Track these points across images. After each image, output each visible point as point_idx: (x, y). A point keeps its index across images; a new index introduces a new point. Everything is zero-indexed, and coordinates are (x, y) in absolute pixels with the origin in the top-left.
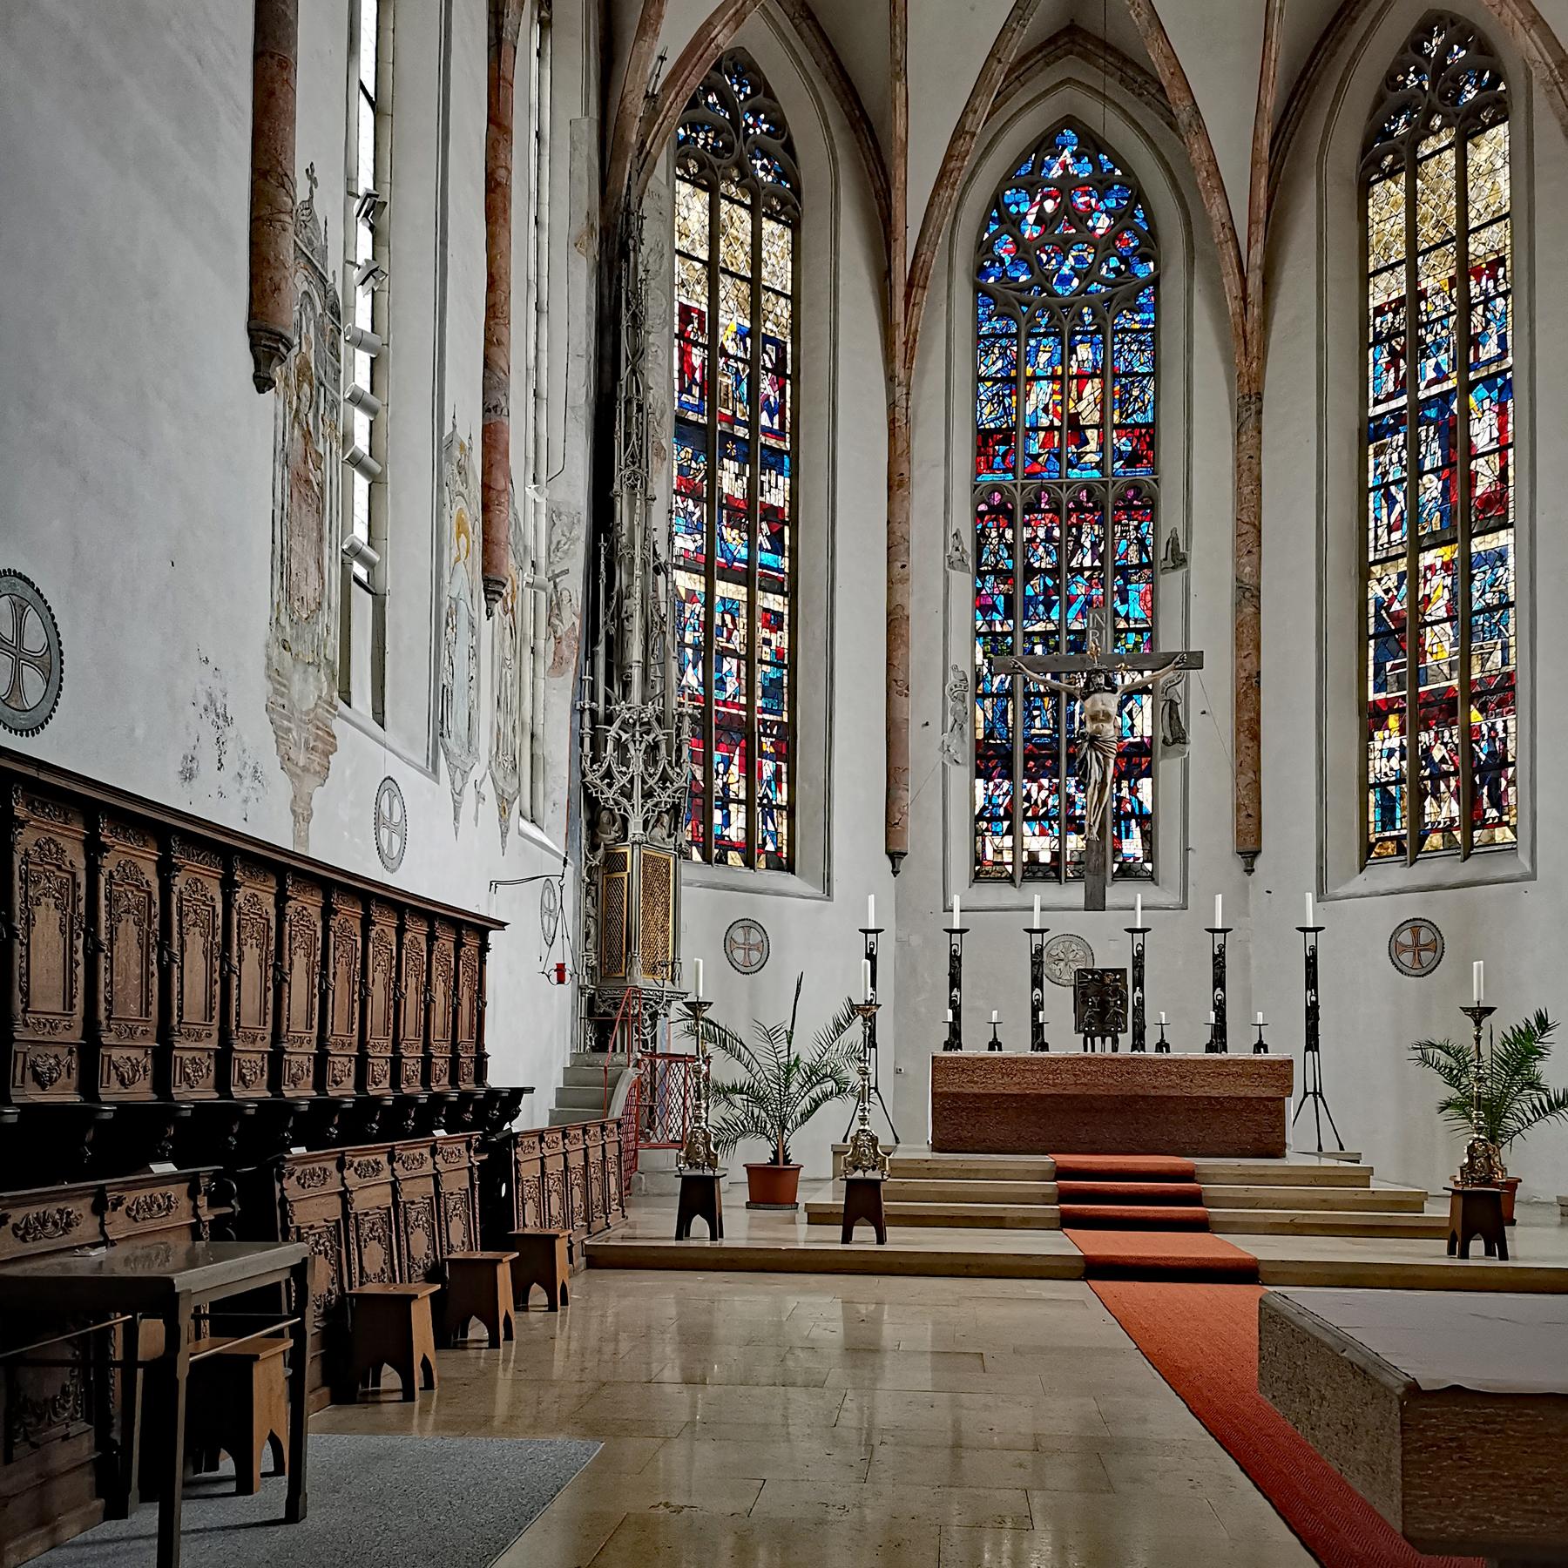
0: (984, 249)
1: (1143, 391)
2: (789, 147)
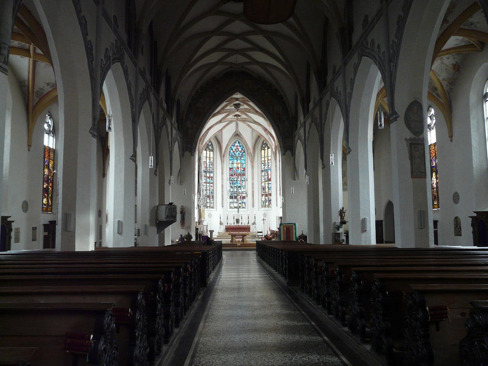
0: (230, 152)
2: (212, 145)
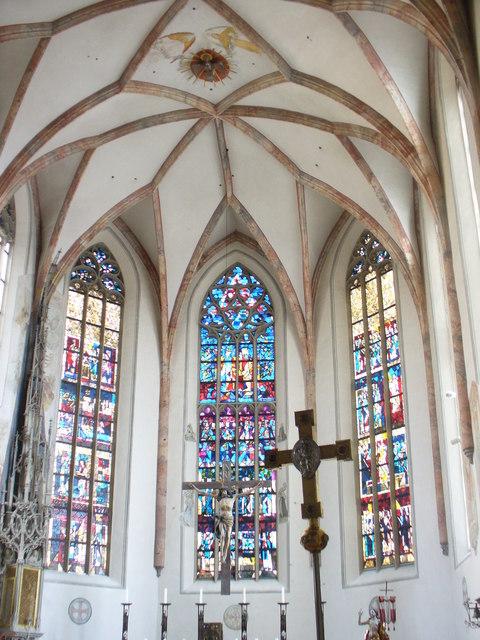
0: (204, 312)
1: (269, 367)
2: (120, 277)
